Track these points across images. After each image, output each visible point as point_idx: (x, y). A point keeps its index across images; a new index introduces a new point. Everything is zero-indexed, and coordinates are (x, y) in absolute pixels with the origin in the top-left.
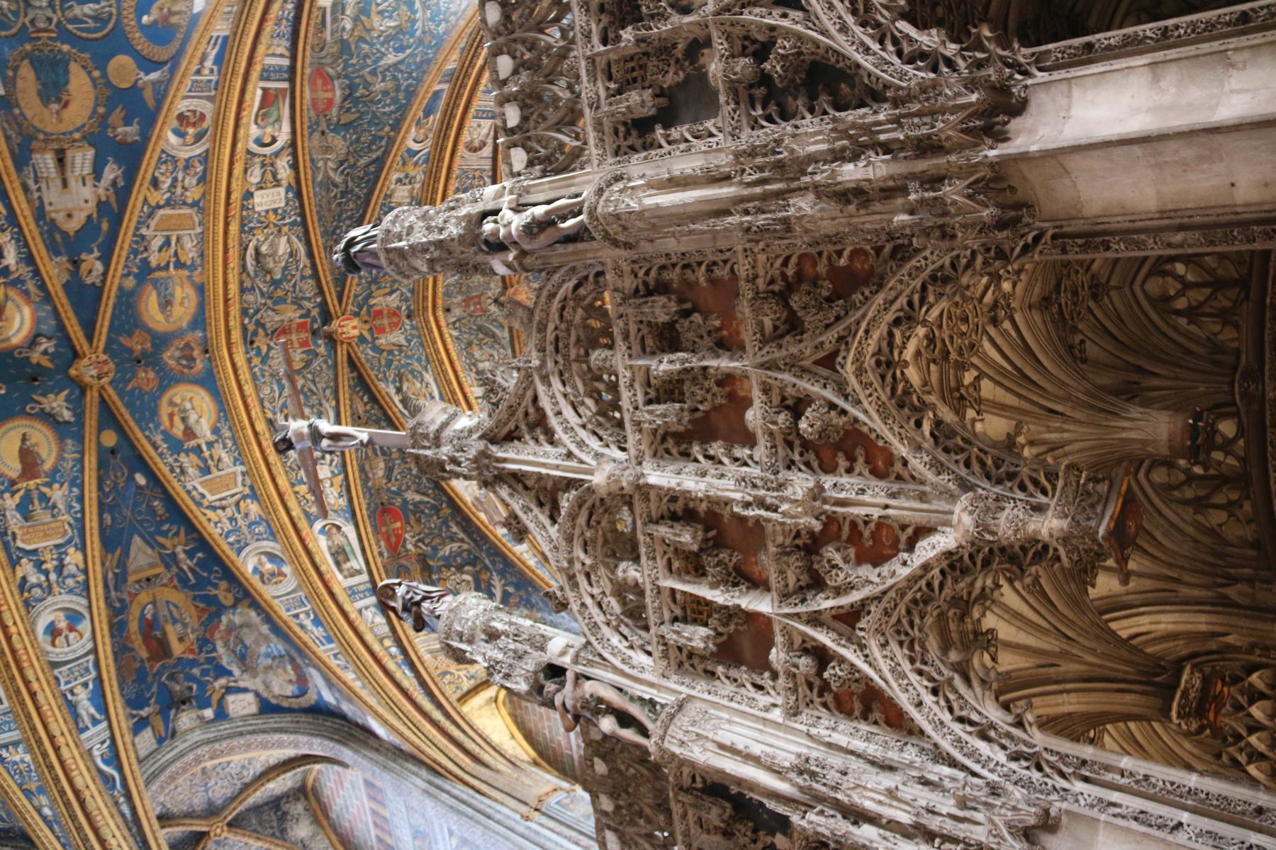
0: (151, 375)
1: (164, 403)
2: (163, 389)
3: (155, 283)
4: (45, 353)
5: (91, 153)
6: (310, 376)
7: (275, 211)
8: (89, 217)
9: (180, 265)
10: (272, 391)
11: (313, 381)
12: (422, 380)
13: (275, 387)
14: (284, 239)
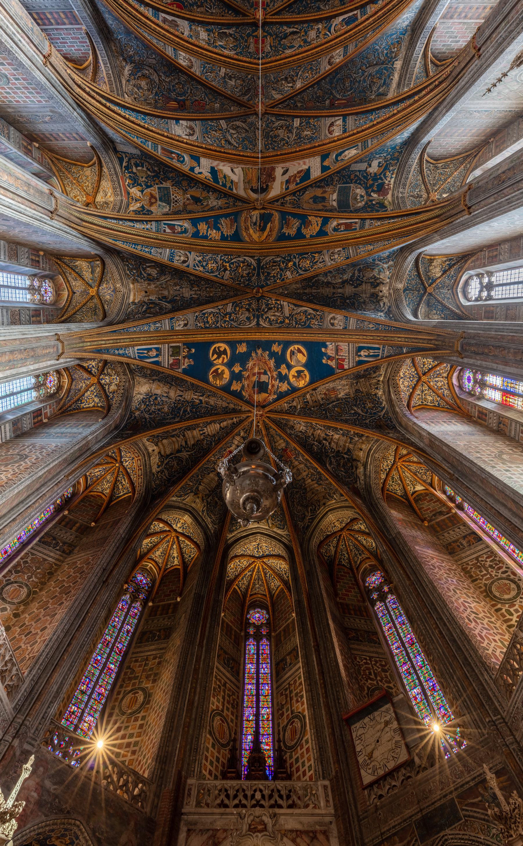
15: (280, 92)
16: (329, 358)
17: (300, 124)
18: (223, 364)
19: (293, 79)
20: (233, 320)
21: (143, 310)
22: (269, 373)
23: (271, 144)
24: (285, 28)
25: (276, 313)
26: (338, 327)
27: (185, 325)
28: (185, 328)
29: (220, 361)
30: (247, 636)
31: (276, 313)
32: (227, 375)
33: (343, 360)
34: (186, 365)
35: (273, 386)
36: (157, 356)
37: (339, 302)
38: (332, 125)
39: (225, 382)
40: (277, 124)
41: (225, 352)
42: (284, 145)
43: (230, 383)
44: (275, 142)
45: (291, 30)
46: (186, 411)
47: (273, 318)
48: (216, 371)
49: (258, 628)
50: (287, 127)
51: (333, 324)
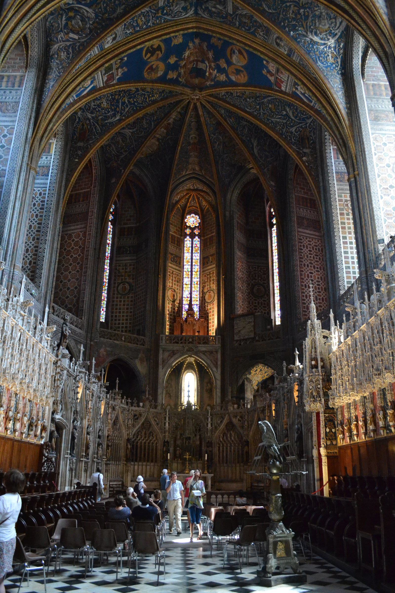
16: (269, 72)
18: (158, 59)
20: (167, 14)
21: (64, 22)
22: (206, 62)
25: (218, 6)
26: (283, 50)
27: (114, 39)
28: (115, 42)
29: (154, 58)
30: (185, 235)
31: (218, 6)
32: (162, 66)
33: (282, 82)
34: (120, 74)
35: (210, 74)
36: (92, 82)
37: (291, 12)
39: (160, 73)
41: (159, 48)
43: (166, 74)
46: (123, 103)
47: (213, 9)
48: (151, 68)
49: (192, 229)
51: (278, 45)
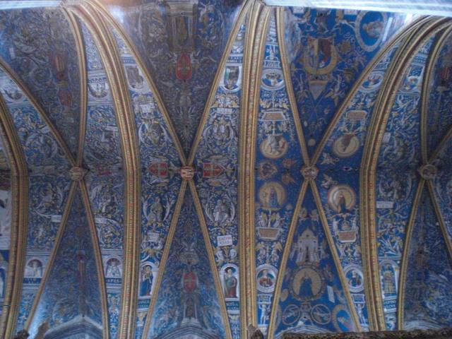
0: (285, 165)
1: (283, 153)
2: (282, 158)
3: (278, 206)
4: (326, 181)
5: (297, 261)
6: (209, 151)
7: (222, 235)
8: (301, 235)
9: (267, 213)
10: (231, 149)
11: (208, 149)
12: (146, 139)
13: (229, 150)
14: (217, 219)
15: (98, 196)
17: (53, 223)
19: (109, 213)
23: (37, 185)
24: (172, 203)
38: (40, 264)
40: (60, 192)
42: (34, 201)
44: (39, 191)
45: (168, 211)
50: (53, 206)
